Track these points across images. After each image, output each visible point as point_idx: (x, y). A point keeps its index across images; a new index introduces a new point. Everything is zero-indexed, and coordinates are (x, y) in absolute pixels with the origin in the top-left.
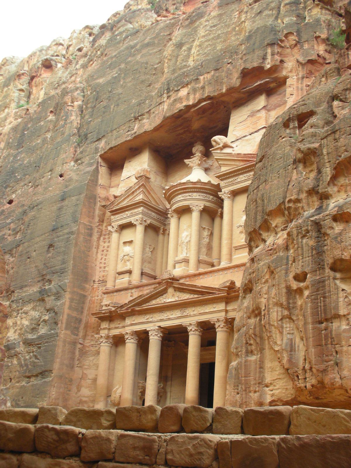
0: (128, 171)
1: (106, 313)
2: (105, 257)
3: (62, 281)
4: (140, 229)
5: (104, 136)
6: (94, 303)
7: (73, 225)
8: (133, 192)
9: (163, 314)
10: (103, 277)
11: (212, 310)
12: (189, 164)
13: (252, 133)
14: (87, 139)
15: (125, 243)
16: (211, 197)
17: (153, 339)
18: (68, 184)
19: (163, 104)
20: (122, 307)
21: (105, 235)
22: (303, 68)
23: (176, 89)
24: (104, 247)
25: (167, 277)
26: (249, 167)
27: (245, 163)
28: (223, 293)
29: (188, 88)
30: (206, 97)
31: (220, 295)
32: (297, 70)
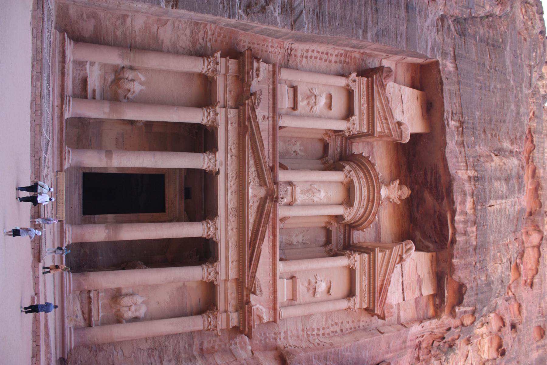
0: (408, 97)
1: (248, 77)
2: (319, 57)
3: (307, 18)
4: (341, 126)
5: (456, 67)
6: (264, 40)
7: (374, 31)
8: (386, 119)
9: (234, 178)
10: (295, 56)
11: (230, 260)
12: (393, 184)
13: (403, 285)
14: (460, 35)
15: (330, 97)
16: (353, 222)
17: (204, 163)
18: (423, 13)
19: (465, 168)
20: (253, 110)
21: (345, 56)
22: (440, 333)
23: (475, 193)
24: (331, 55)
26: (374, 293)
27: (379, 288)
29: (471, 209)
30: (455, 238)
31: (246, 277)
32: (441, 327)
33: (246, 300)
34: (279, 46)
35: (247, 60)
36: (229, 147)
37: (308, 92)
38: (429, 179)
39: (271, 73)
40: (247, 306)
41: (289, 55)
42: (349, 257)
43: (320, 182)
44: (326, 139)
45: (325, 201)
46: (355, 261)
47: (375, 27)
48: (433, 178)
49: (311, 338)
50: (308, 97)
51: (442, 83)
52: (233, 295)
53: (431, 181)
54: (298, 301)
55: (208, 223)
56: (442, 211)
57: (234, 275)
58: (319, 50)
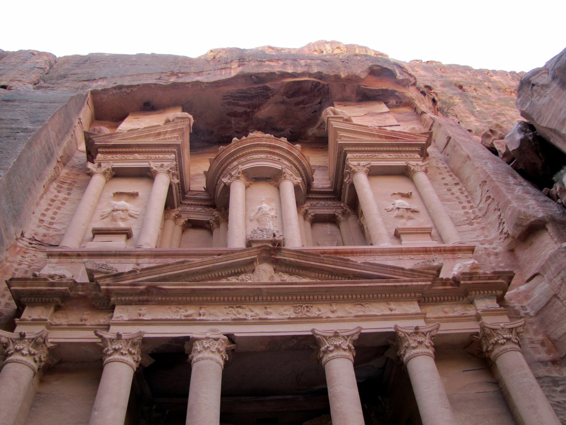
1: (60, 284)
8: (159, 134)
9: (240, 310)
10: (45, 235)
15: (119, 195)
17: (211, 359)
25: (265, 238)
26: (398, 145)
28: (423, 281)
30: (316, 73)
31: (414, 283)
33: (452, 285)
34: (22, 254)
35: (28, 288)
36: (183, 318)
37: (105, 220)
38: (240, 110)
39: (64, 260)
40: (462, 282)
41: (41, 243)
42: (354, 172)
43: (246, 211)
44: (182, 221)
45: (274, 205)
46: (359, 165)
47: (22, 122)
48: (241, 102)
49: (480, 214)
50: (114, 219)
51: (120, 87)
52: (447, 309)
53: (244, 106)
54: (430, 225)
55: (326, 351)
56: (282, 90)
57: (412, 306)
58: (45, 208)
